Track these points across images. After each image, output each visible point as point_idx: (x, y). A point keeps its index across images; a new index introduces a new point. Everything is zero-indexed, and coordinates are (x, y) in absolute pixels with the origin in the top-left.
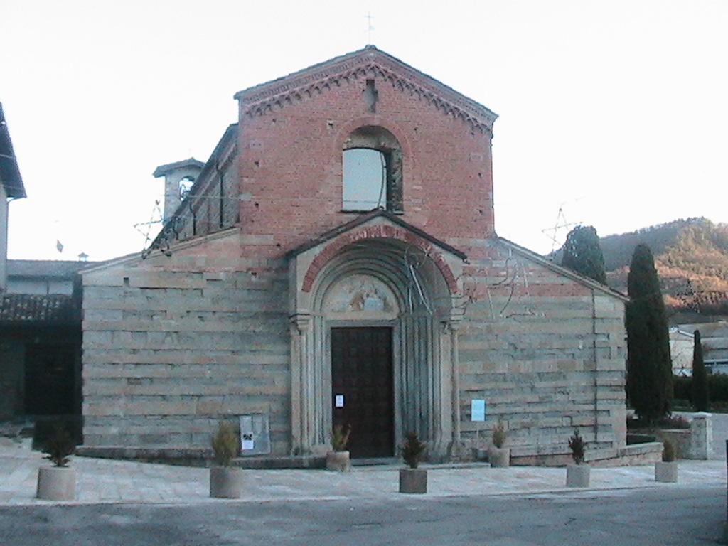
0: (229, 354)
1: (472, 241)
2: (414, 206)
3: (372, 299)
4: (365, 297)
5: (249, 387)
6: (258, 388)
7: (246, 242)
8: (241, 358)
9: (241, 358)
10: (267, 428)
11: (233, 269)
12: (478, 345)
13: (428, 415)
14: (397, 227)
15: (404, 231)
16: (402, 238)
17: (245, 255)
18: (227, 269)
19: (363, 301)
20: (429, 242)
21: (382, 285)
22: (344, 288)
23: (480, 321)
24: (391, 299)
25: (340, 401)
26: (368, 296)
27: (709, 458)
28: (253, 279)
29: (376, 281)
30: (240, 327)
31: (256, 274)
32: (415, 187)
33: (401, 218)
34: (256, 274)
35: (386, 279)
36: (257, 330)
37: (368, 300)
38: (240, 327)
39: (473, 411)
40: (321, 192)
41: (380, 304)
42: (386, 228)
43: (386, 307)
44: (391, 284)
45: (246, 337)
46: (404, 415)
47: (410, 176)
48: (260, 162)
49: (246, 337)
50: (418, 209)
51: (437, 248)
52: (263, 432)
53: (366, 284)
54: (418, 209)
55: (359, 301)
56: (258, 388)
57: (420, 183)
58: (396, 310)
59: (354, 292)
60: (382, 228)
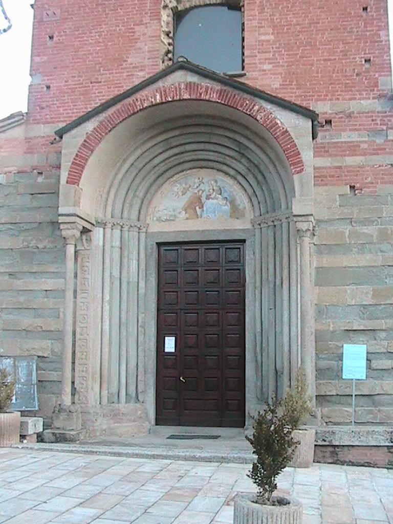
0: (7, 277)
1: (353, 103)
2: (260, 63)
3: (215, 201)
4: (203, 199)
5: (27, 321)
6: (38, 322)
7: (32, 134)
8: (20, 282)
9: (19, 283)
10: (34, 373)
11: (14, 169)
12: (365, 260)
13: (283, 368)
14: (206, 83)
15: (218, 87)
16: (214, 97)
17: (30, 151)
18: (7, 169)
19: (199, 205)
20: (257, 100)
21: (229, 181)
22: (175, 189)
23: (366, 222)
24: (242, 200)
25: (170, 345)
26: (208, 197)
27: (36, 358)
28: (40, 179)
29: (220, 177)
30: (20, 242)
31: (42, 173)
32: (263, 38)
33: (242, 80)
34: (42, 173)
35: (232, 172)
36: (41, 246)
37: (208, 204)
38: (20, 242)
39: (346, 363)
40: (129, 61)
41: (227, 208)
42: (189, 86)
43: (236, 212)
44: (239, 178)
45: (27, 254)
46: (259, 367)
47: (255, 23)
48: (55, 36)
49: (27, 254)
50: (267, 67)
51: (269, 107)
52: (29, 380)
53: (204, 181)
54: (267, 67)
55: (195, 205)
56: (38, 322)
57: (271, 31)
58: (249, 215)
59: (189, 194)
60: (183, 86)
